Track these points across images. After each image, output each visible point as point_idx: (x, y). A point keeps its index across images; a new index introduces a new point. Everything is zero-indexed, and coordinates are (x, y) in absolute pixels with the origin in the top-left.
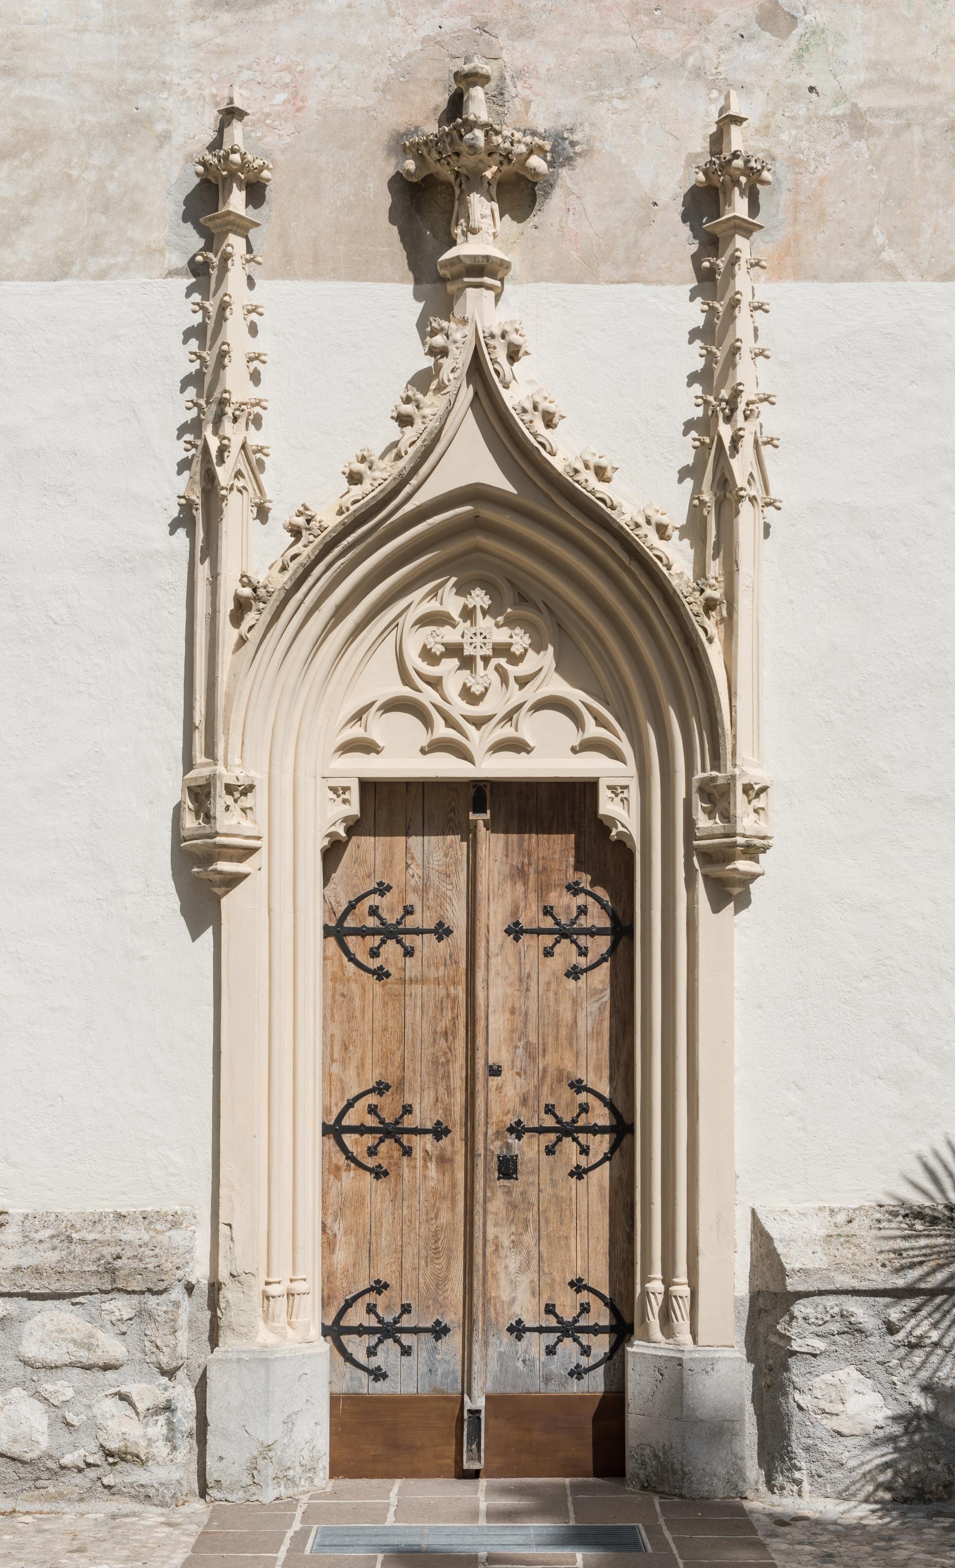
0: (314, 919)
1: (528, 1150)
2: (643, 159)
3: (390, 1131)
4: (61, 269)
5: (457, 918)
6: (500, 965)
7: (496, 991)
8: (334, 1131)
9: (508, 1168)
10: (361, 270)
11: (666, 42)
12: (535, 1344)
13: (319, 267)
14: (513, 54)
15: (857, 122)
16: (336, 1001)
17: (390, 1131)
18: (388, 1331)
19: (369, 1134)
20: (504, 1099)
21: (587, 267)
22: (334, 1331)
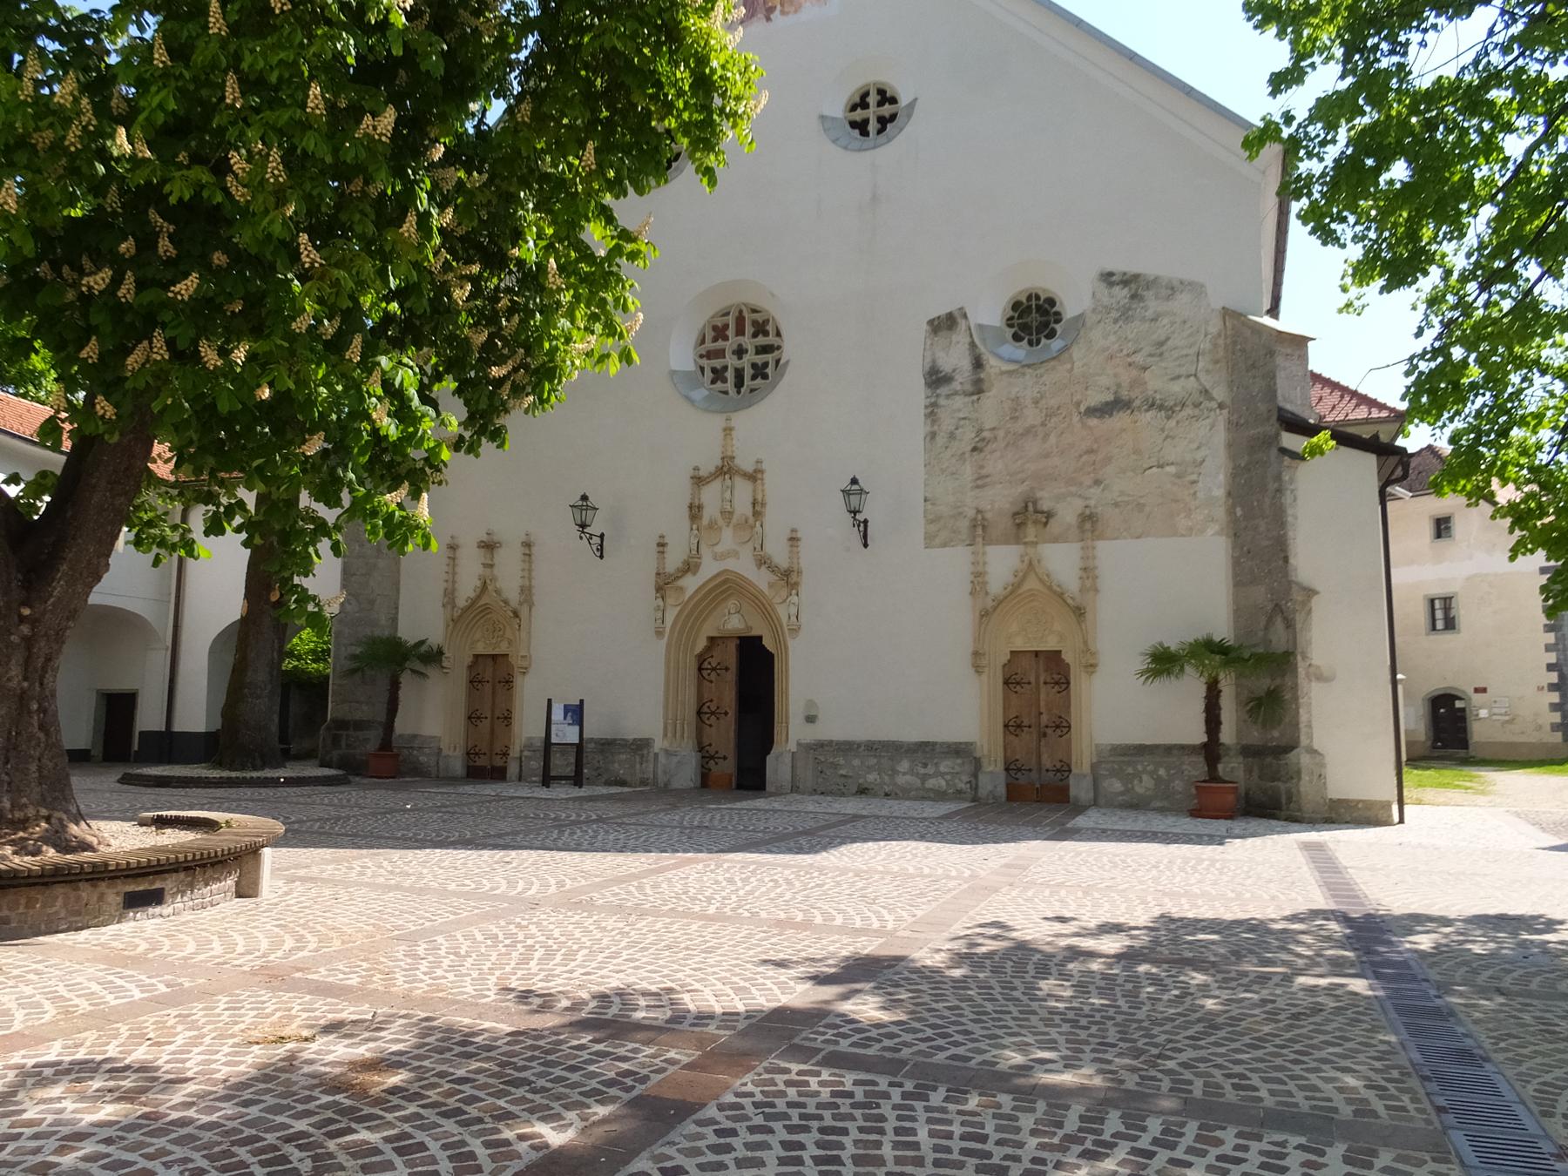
0: (1000, 681)
1: (1049, 731)
2: (1068, 514)
3: (1019, 726)
4: (944, 545)
5: (1033, 680)
6: (1043, 689)
7: (1043, 696)
8: (1006, 726)
9: (1045, 735)
10: (1007, 542)
11: (1073, 489)
12: (1051, 774)
13: (998, 542)
14: (1039, 494)
15: (1116, 505)
16: (1006, 699)
17: (1019, 726)
18: (1019, 770)
19: (1013, 727)
20: (1044, 719)
21: (1055, 540)
22: (1007, 769)
